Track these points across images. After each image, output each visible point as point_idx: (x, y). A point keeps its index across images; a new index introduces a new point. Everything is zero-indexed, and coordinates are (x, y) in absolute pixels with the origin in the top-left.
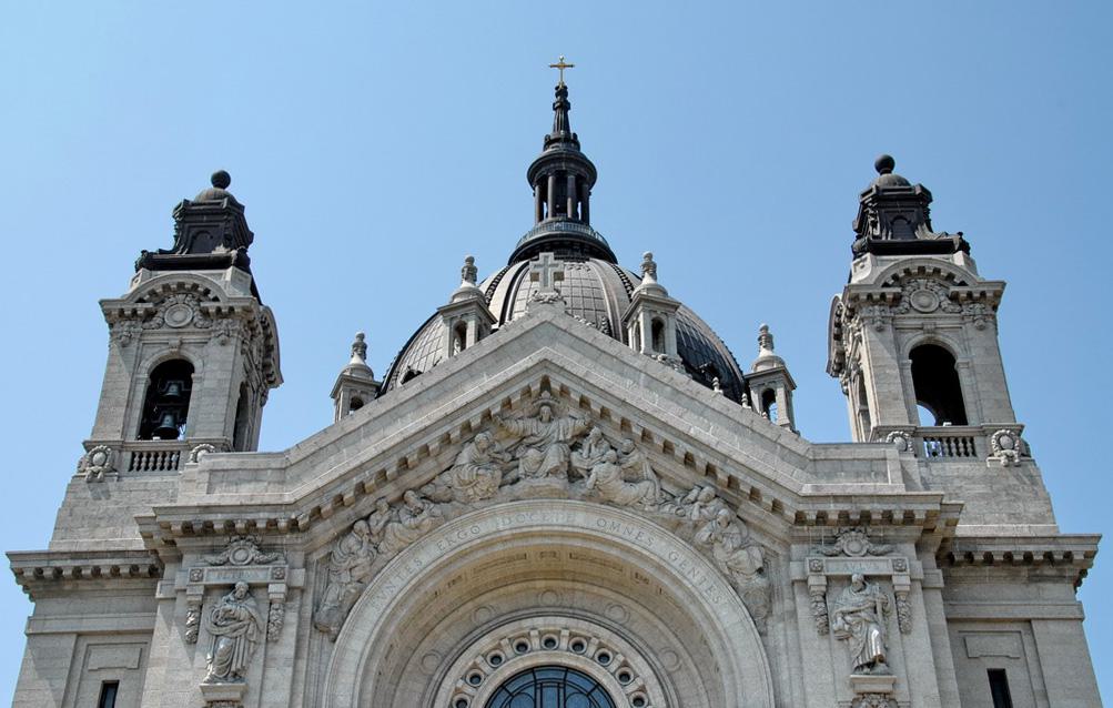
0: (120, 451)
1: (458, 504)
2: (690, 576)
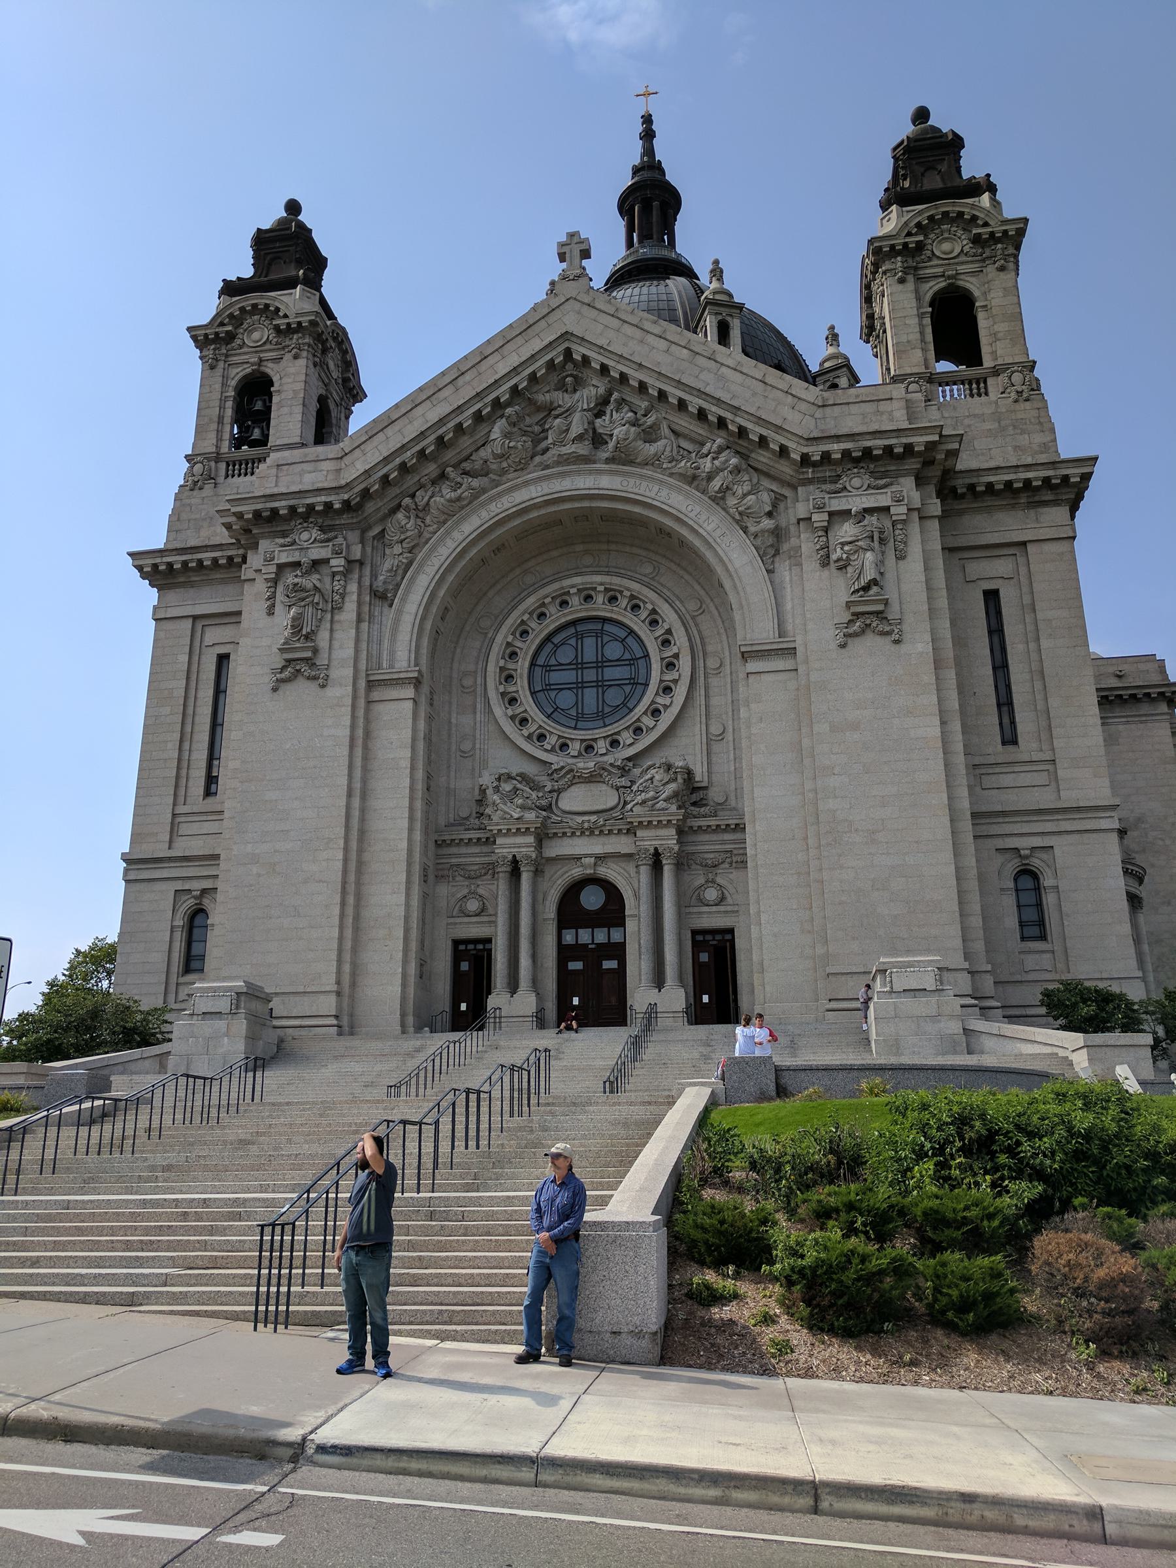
0: (216, 462)
2: (705, 525)
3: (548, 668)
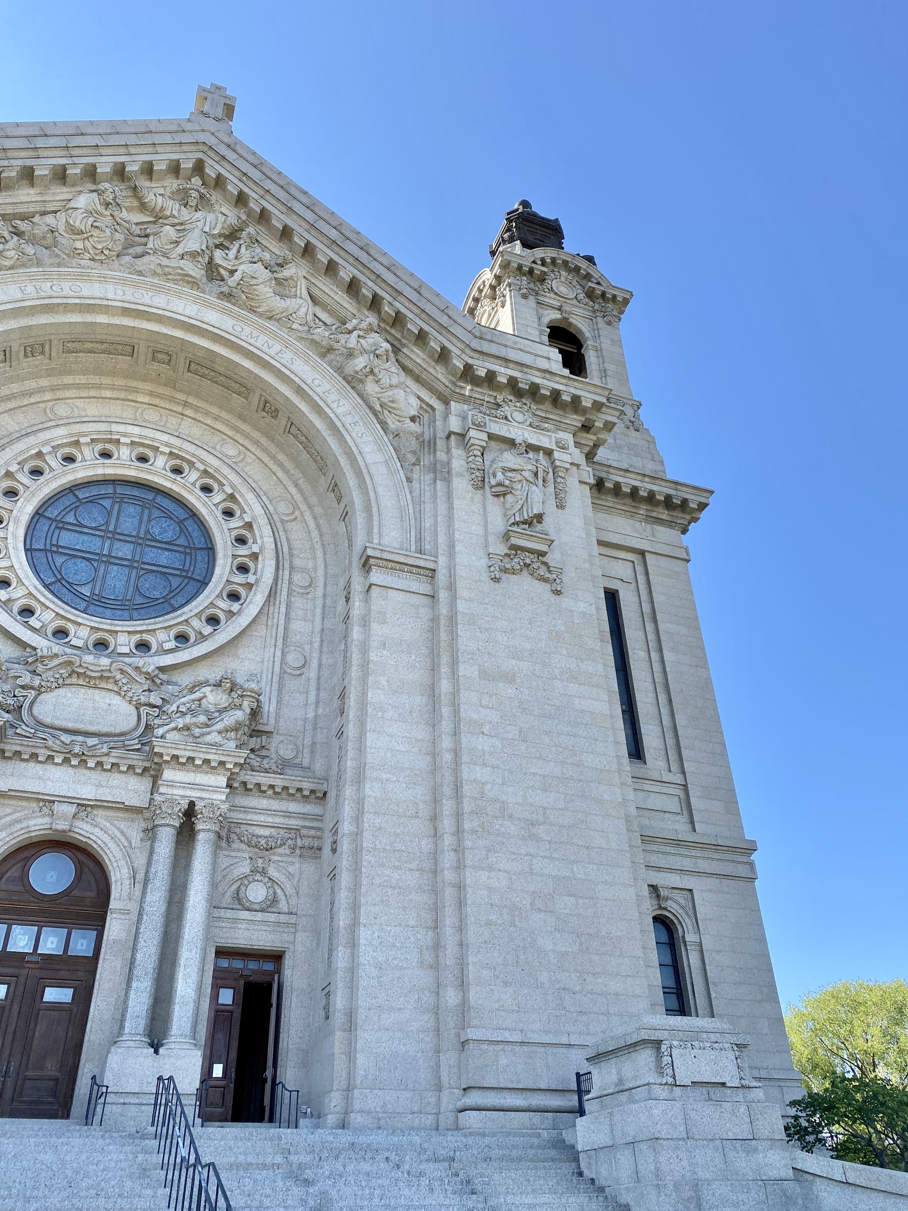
1: (60, 253)
2: (334, 406)
3: (61, 525)
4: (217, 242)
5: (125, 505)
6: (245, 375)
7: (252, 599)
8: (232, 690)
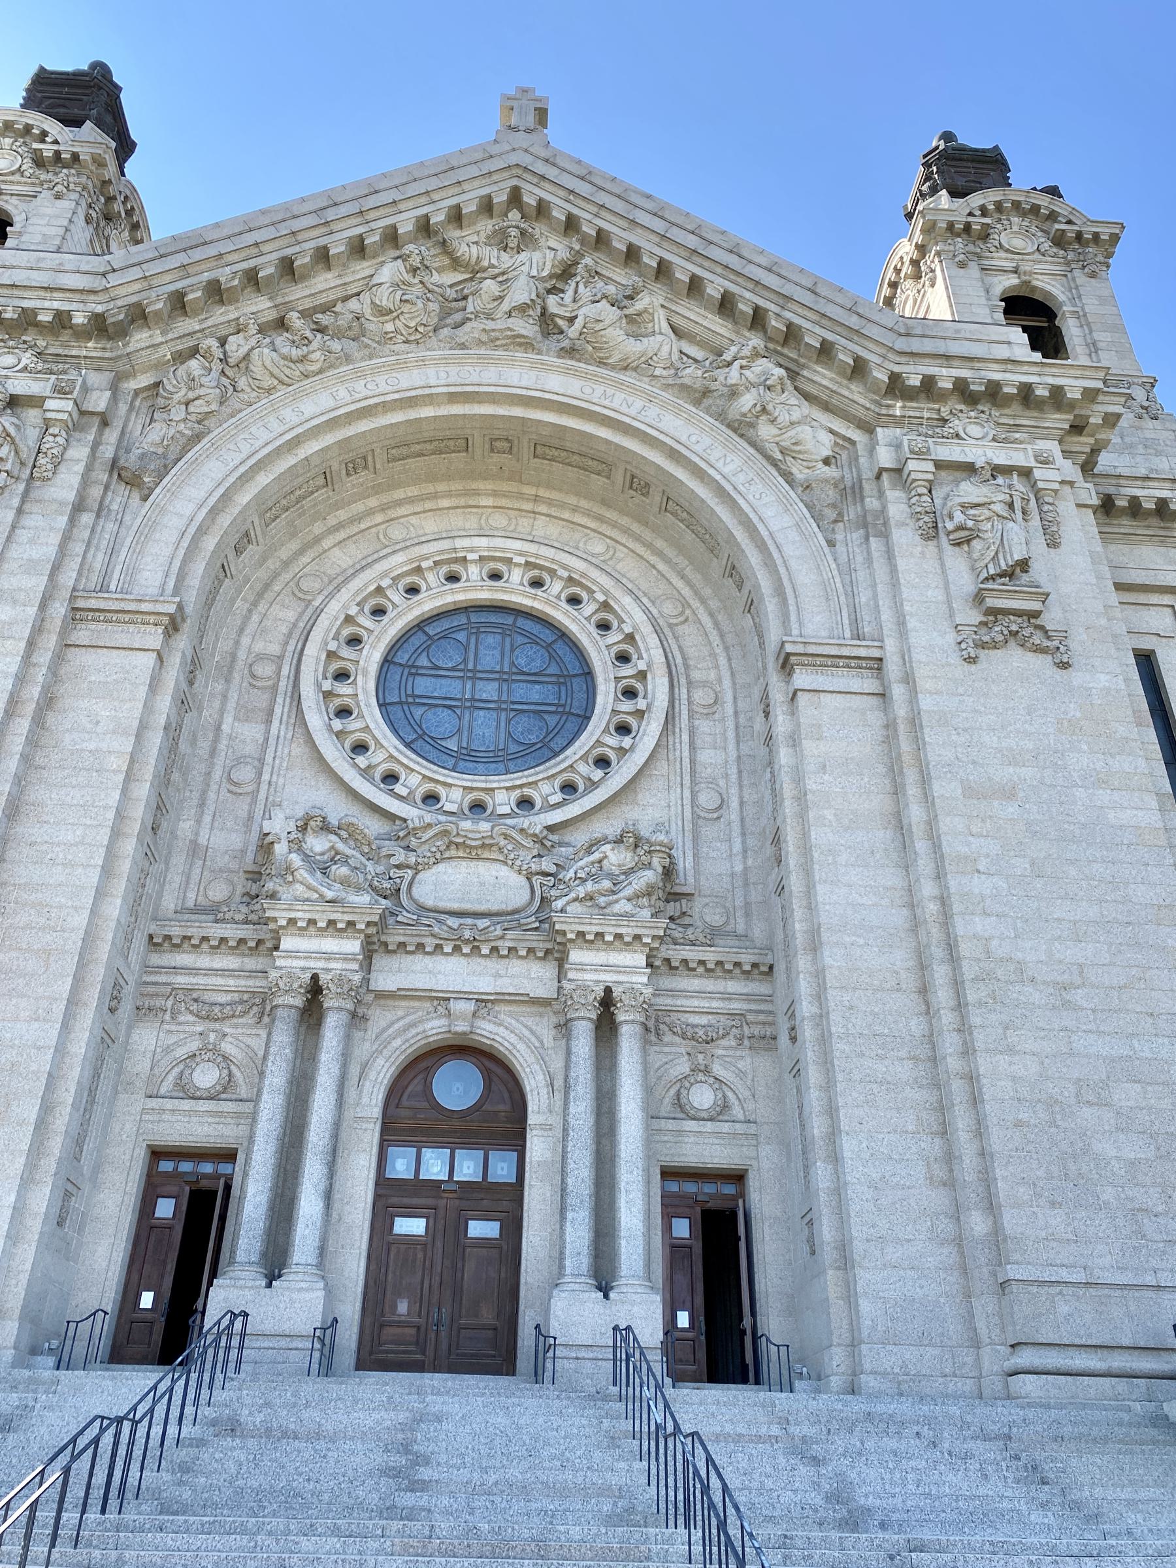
2: (719, 465)
3: (413, 671)
4: (548, 286)
5: (482, 636)
6: (603, 448)
7: (645, 730)
8: (636, 846)
